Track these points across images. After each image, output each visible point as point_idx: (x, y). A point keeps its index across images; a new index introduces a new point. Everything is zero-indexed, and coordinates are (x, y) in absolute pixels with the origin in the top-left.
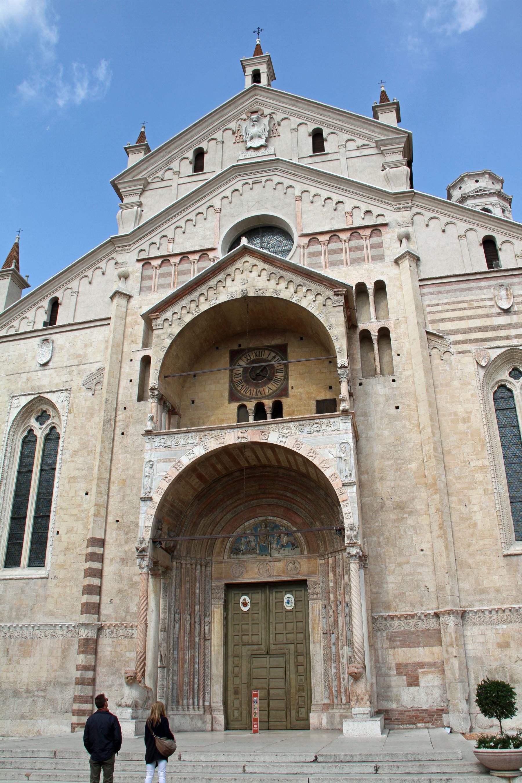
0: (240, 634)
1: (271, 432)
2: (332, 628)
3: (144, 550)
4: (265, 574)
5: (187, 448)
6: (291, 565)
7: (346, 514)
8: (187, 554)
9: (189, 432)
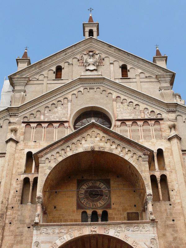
1: (111, 229)
9: (61, 225)
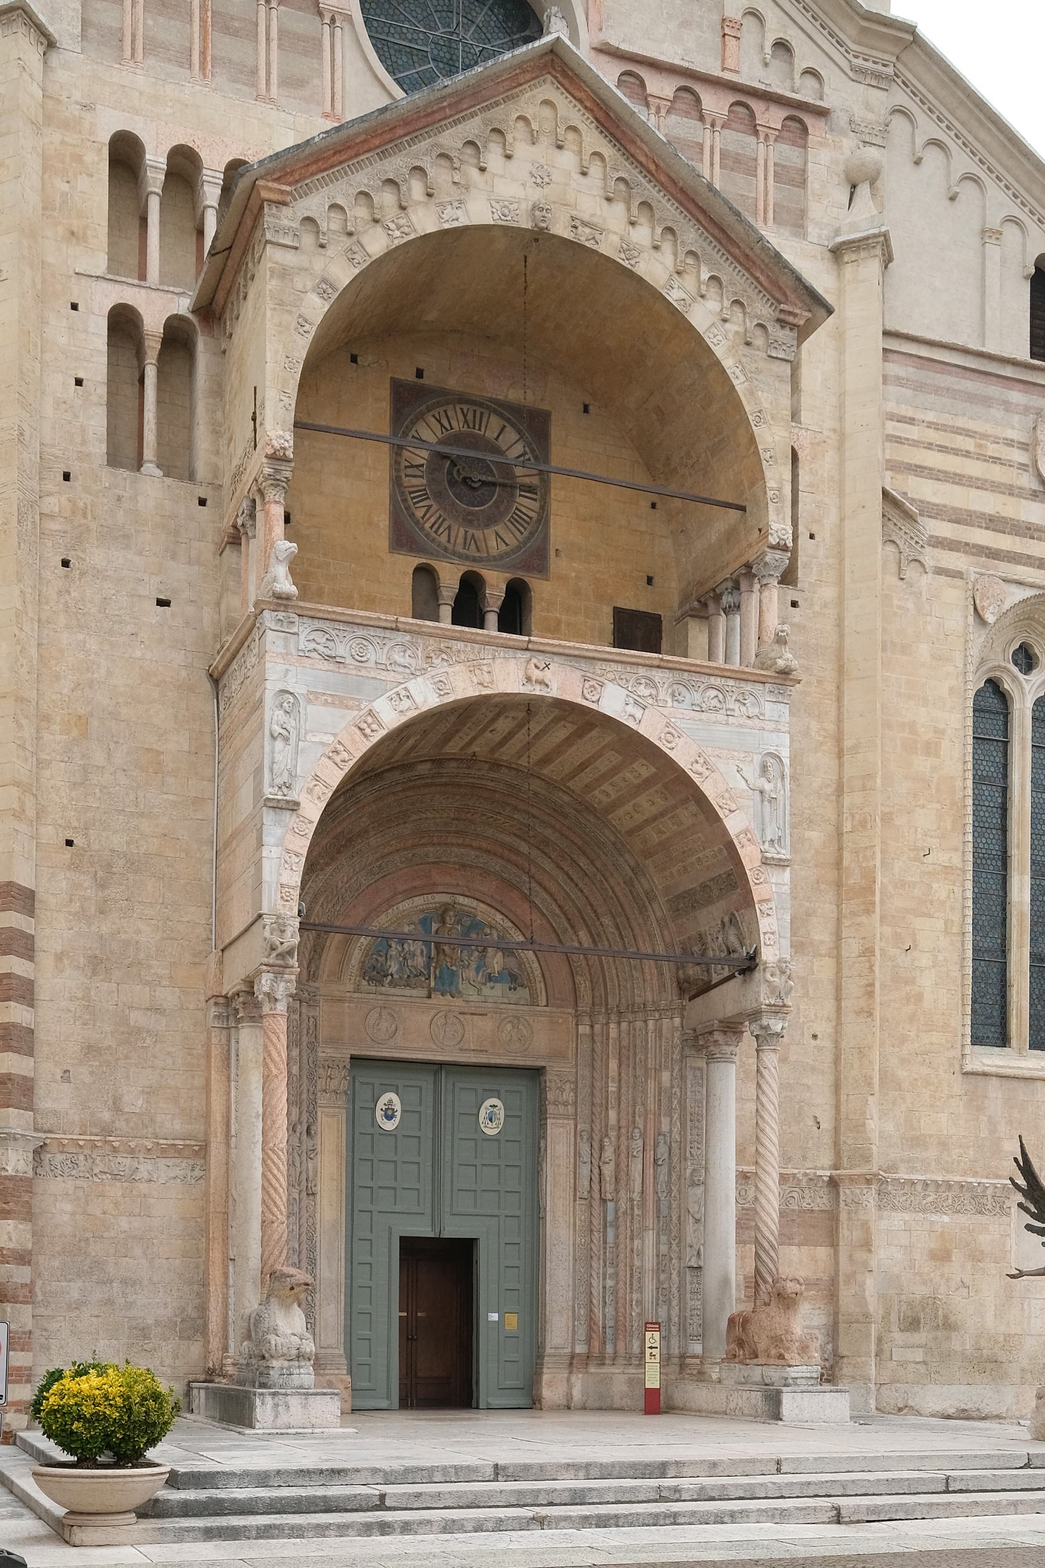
5: (391, 676)
7: (765, 933)
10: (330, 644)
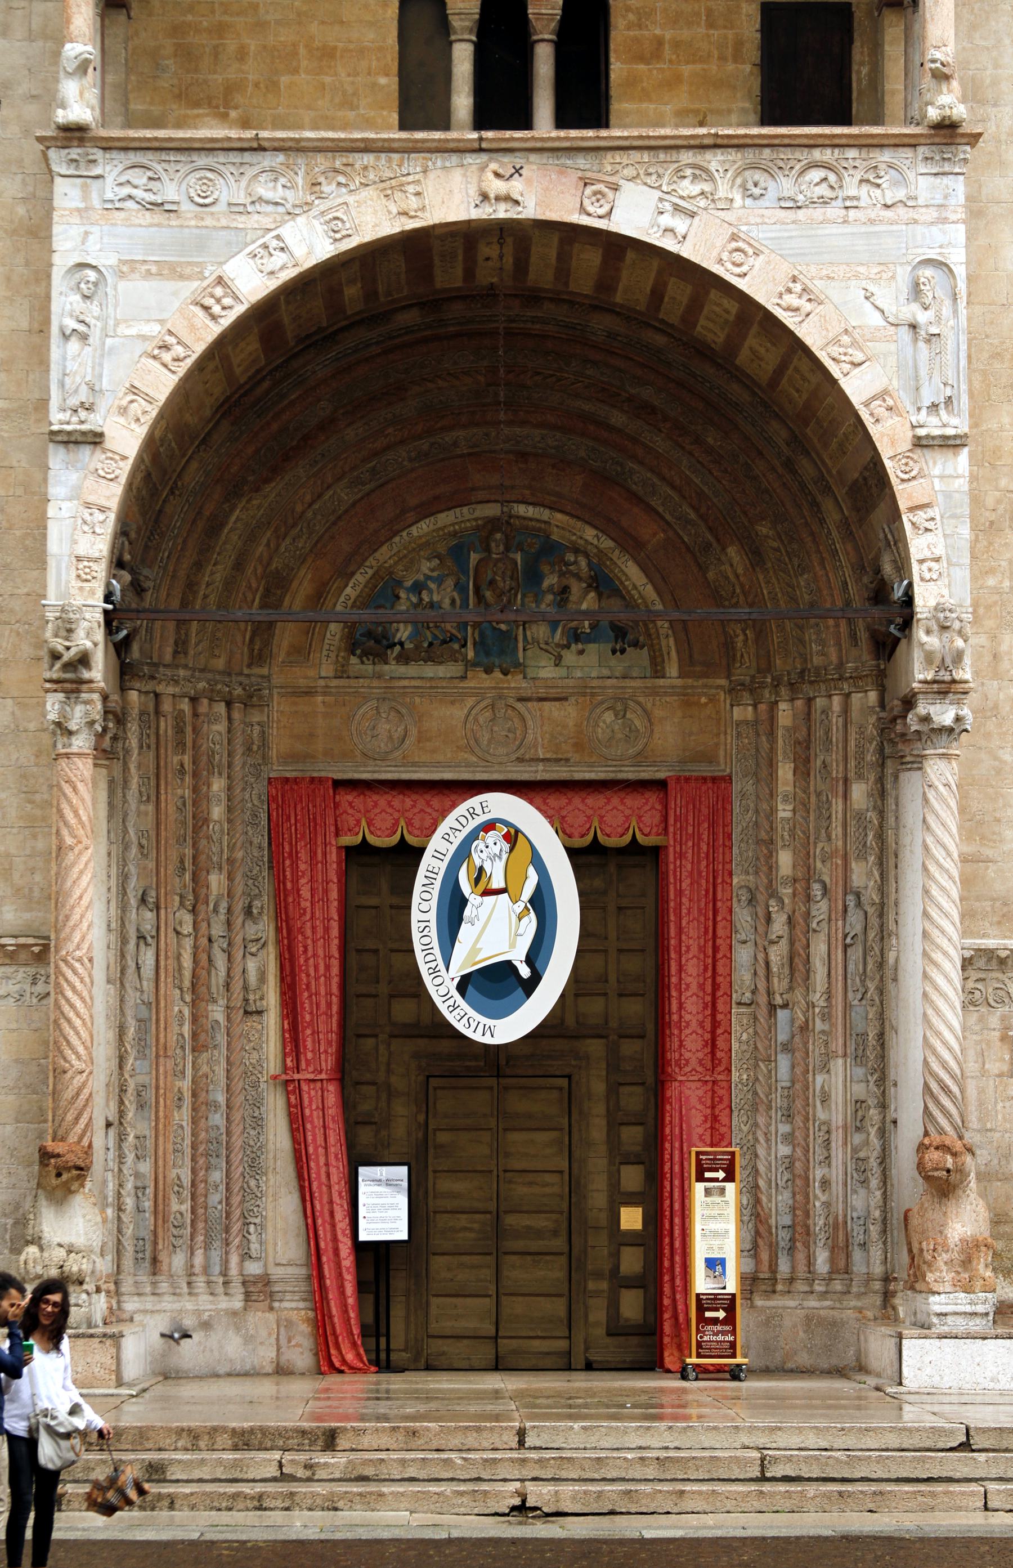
0: (383, 989)
1: (627, 186)
2: (779, 985)
3: (84, 660)
4: (502, 750)
5: (254, 221)
6: (609, 717)
7: (921, 562)
8: (176, 652)
9: (262, 149)
10: (152, 185)
